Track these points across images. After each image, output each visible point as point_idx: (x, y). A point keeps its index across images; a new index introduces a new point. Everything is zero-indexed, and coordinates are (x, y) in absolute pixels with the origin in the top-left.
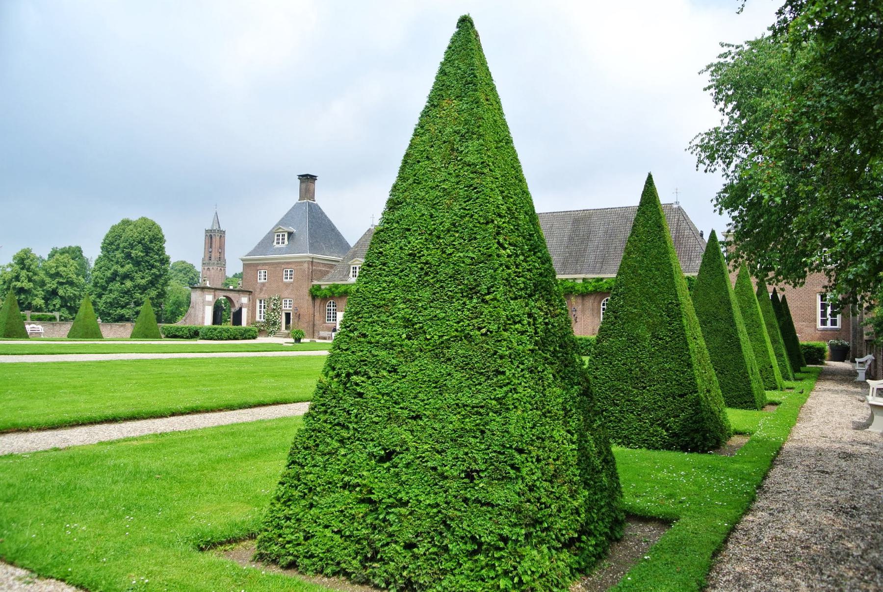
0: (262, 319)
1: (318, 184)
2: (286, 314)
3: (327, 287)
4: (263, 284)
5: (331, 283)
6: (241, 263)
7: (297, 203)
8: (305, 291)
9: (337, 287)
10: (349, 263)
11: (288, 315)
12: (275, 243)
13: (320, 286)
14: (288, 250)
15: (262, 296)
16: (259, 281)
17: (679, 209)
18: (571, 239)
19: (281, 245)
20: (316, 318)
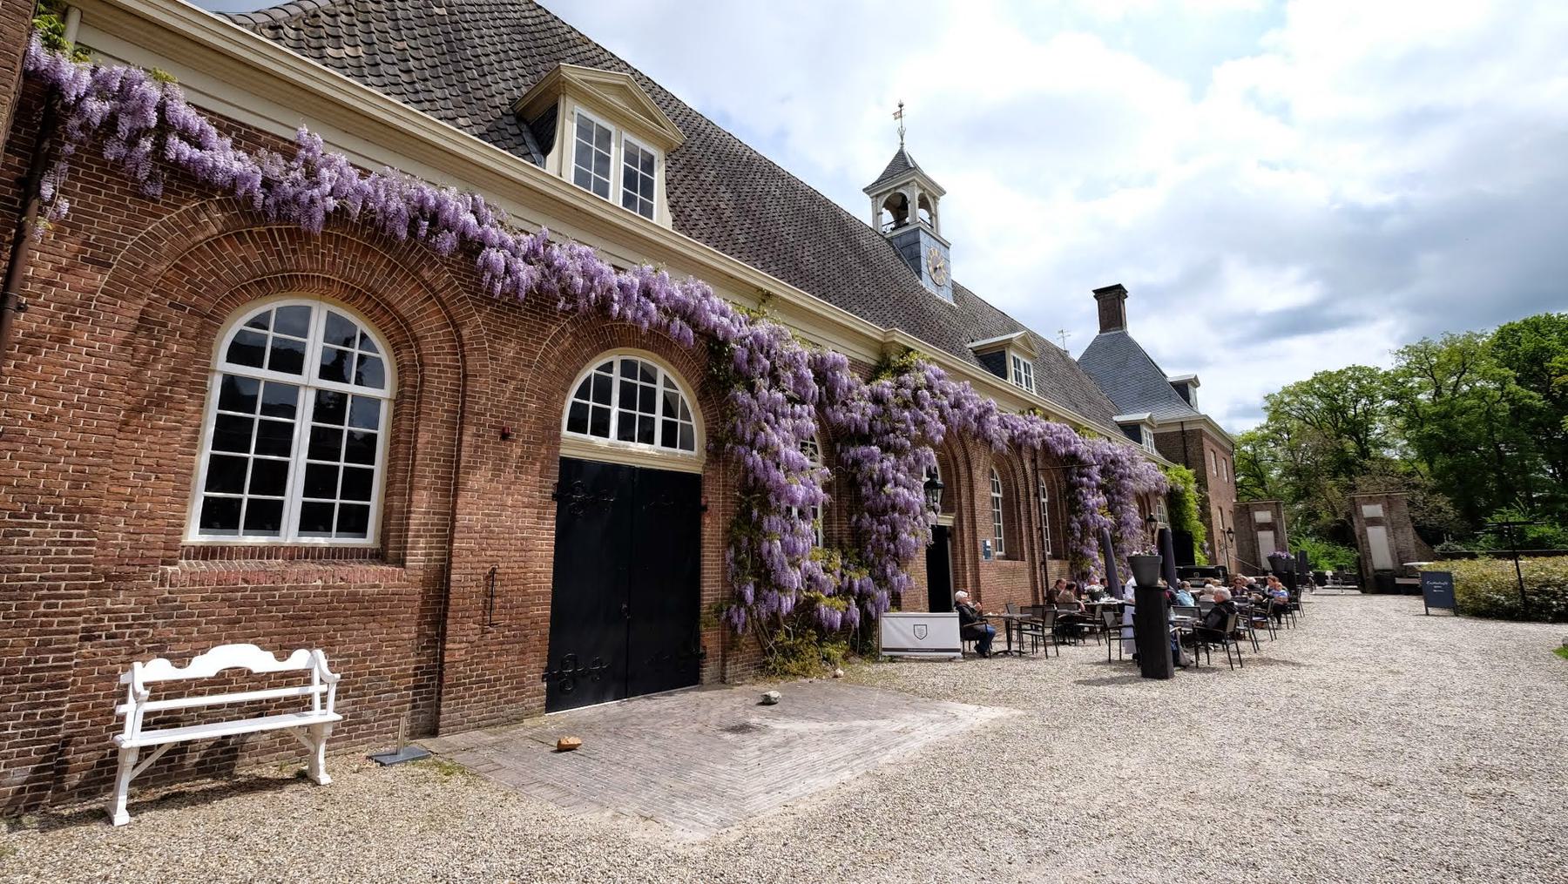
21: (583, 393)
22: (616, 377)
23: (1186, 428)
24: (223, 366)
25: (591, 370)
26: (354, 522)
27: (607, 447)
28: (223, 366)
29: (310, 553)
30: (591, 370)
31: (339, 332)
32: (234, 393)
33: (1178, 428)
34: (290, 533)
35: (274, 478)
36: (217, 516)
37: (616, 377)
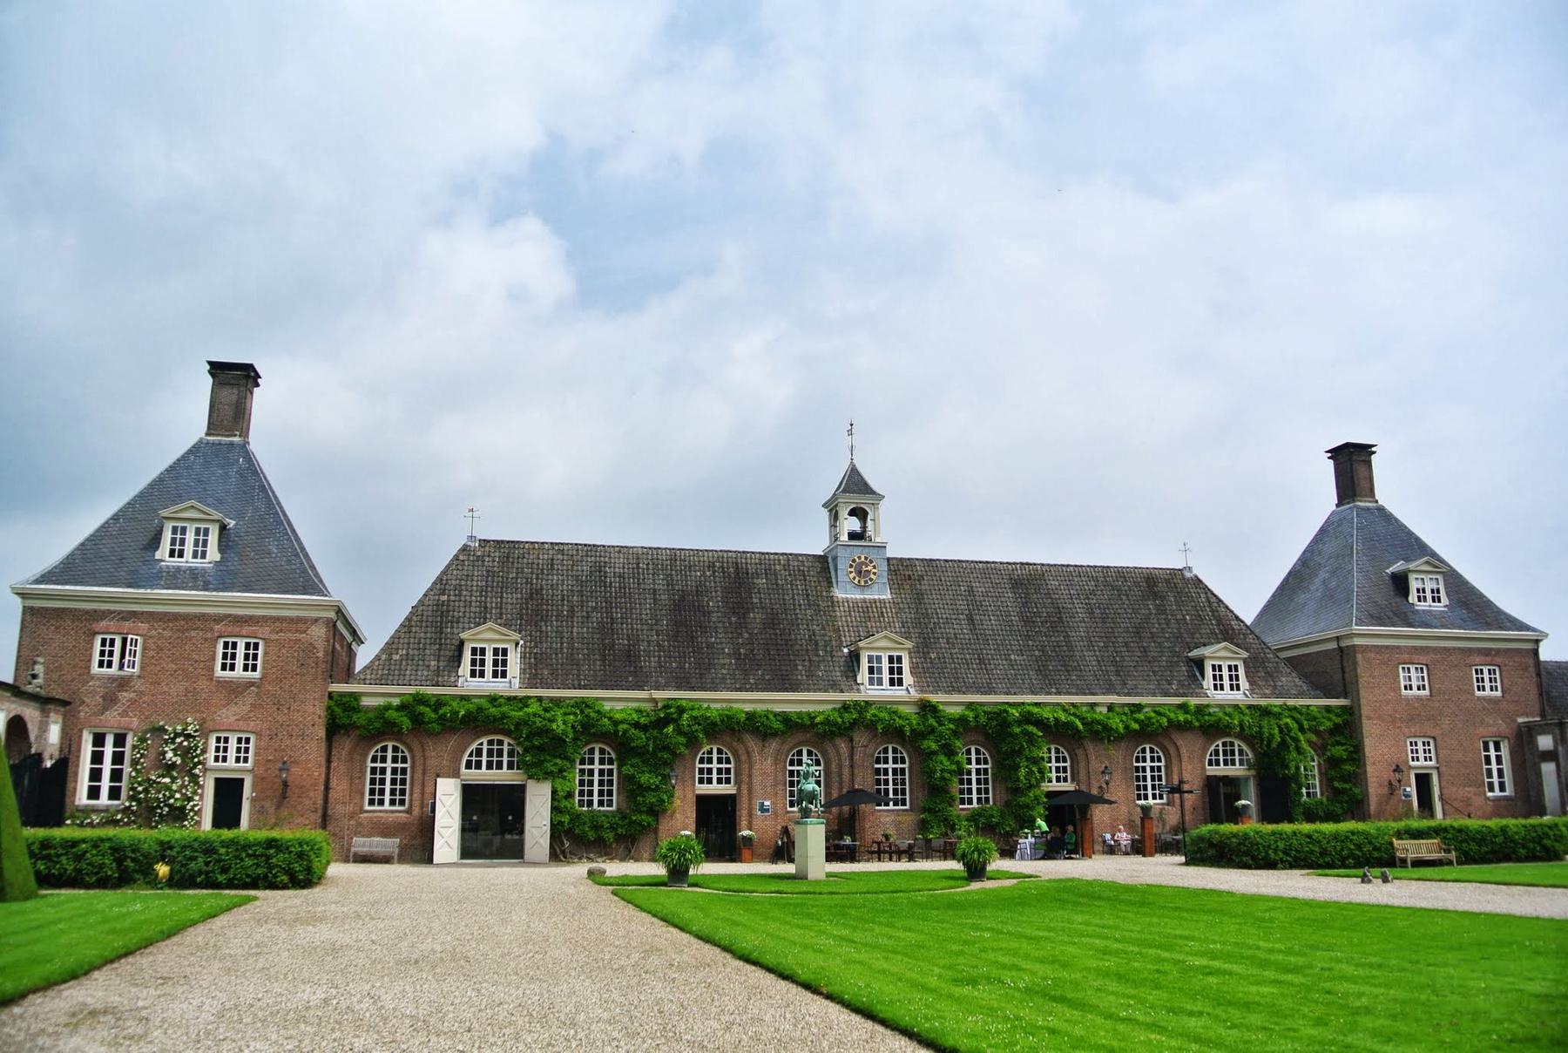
0: (104, 799)
1: (262, 401)
2: (220, 784)
3: (396, 702)
4: (123, 683)
5: (411, 690)
6: (18, 603)
7: (201, 441)
8: (314, 713)
9: (439, 703)
10: (463, 636)
11: (228, 792)
12: (163, 552)
13: (356, 696)
14: (224, 578)
15: (112, 720)
16: (95, 669)
17: (1198, 581)
18: (1027, 621)
19: (188, 560)
20: (332, 794)
21: (471, 755)
22: (485, 748)
23: (1344, 644)
24: (370, 765)
25: (474, 746)
26: (402, 802)
27: (484, 775)
28: (370, 765)
29: (392, 812)
30: (474, 746)
31: (395, 749)
32: (374, 770)
33: (1333, 645)
34: (387, 806)
35: (382, 792)
36: (372, 802)
37: (485, 748)
